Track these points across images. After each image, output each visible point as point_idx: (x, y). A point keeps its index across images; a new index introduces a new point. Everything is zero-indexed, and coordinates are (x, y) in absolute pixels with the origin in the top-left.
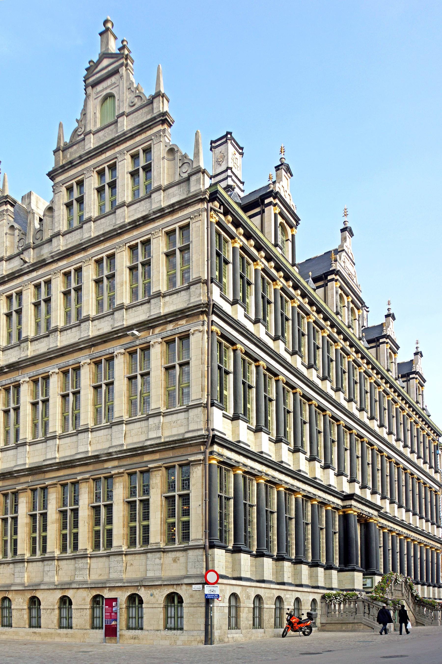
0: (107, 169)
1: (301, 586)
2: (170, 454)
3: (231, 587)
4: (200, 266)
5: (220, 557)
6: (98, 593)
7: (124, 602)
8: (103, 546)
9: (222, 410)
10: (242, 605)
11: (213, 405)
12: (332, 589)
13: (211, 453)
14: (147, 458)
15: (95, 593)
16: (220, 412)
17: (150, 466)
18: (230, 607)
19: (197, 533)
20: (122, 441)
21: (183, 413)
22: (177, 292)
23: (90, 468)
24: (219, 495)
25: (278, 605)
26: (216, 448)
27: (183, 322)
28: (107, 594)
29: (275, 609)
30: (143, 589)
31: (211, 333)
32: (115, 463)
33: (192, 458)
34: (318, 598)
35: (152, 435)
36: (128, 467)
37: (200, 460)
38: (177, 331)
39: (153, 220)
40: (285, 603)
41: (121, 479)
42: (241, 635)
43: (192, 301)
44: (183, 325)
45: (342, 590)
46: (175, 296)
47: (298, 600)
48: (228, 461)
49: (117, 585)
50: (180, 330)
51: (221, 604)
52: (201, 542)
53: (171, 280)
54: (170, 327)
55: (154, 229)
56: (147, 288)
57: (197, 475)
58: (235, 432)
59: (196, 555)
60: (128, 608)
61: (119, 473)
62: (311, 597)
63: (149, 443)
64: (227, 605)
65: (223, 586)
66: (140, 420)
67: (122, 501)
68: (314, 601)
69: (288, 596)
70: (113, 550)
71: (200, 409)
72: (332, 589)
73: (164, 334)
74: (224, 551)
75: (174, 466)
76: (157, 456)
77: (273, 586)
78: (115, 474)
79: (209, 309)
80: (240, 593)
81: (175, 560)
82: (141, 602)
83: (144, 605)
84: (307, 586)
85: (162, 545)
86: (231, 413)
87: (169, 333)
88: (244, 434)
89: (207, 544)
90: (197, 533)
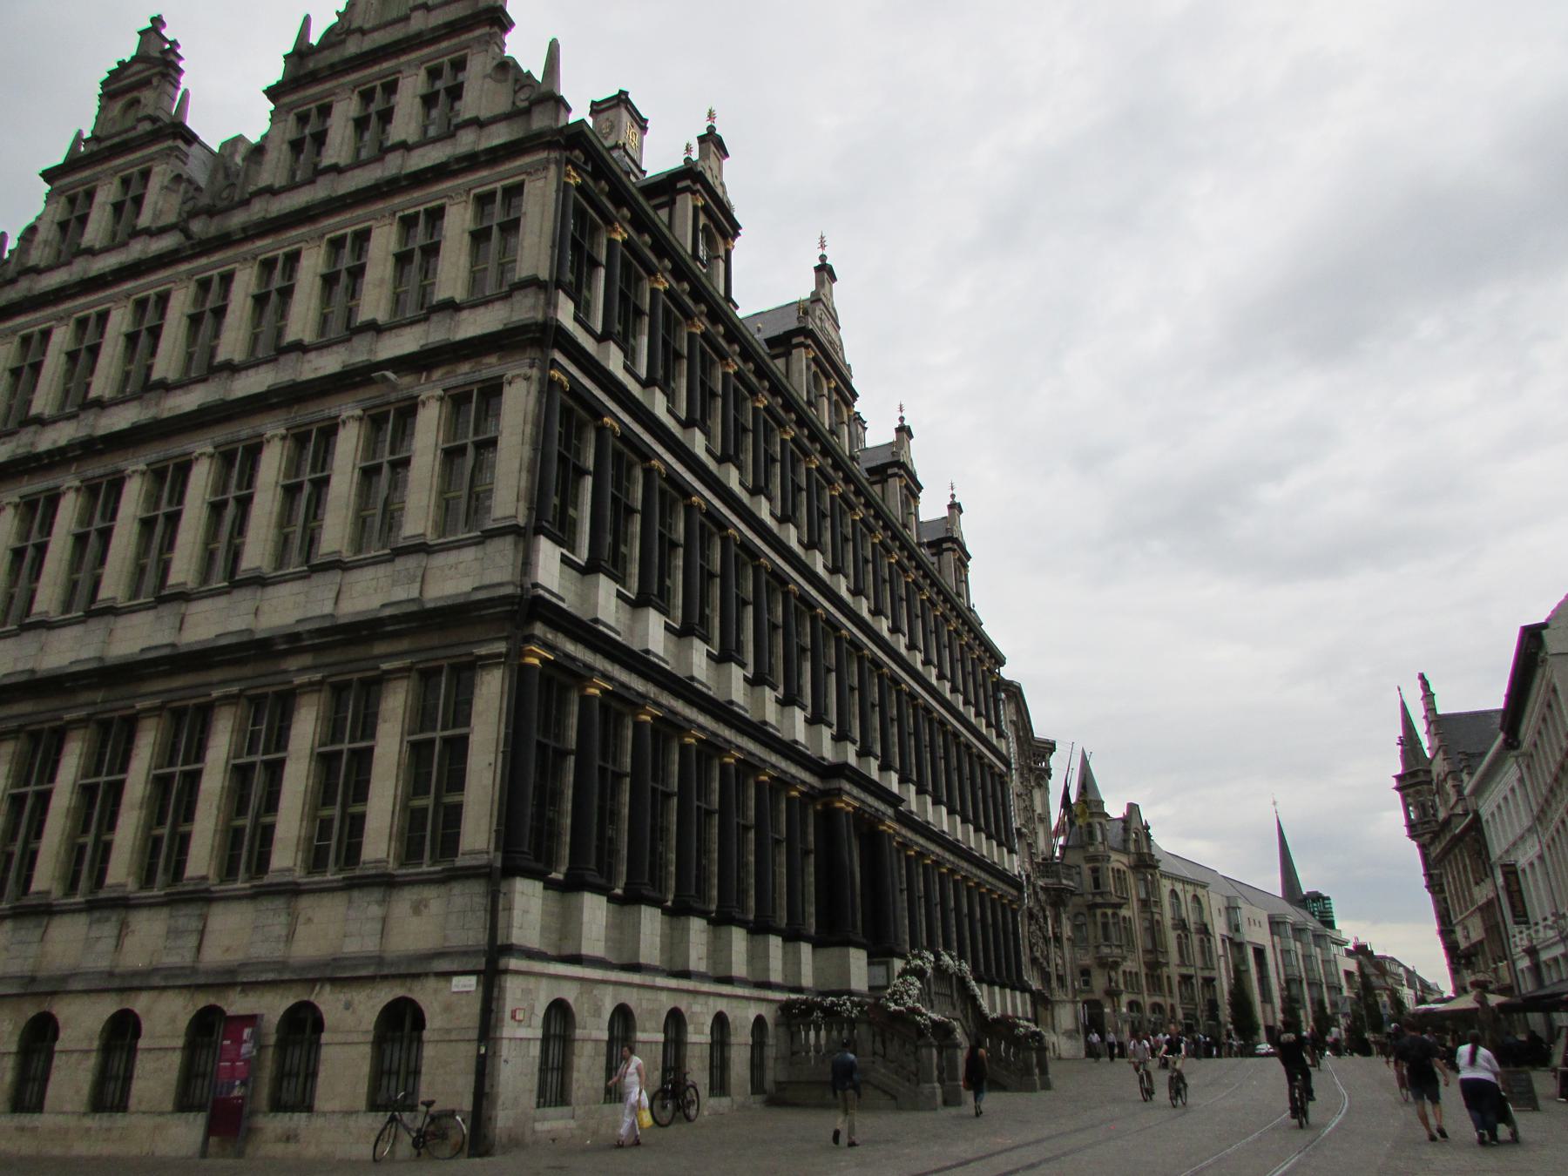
0: (379, 89)
1: (728, 980)
2: (434, 639)
3: (554, 983)
4: (534, 251)
5: (529, 903)
6: (212, 1000)
7: (273, 1029)
8: (248, 868)
9: (561, 545)
10: (579, 1033)
11: (539, 531)
12: (799, 990)
13: (530, 639)
14: (380, 648)
15: (203, 1001)
16: (558, 551)
17: (385, 666)
18: (546, 1040)
19: (477, 834)
20: (328, 608)
21: (473, 549)
22: (486, 302)
23: (247, 671)
24: (539, 743)
25: (672, 1034)
26: (539, 629)
27: (493, 360)
28: (237, 1004)
29: (665, 1044)
30: (328, 988)
31: (549, 386)
32: (307, 660)
33: (483, 651)
34: (768, 1013)
35: (400, 594)
36: (333, 670)
37: (499, 655)
38: (477, 376)
39: (454, 174)
40: (690, 1028)
41: (315, 697)
42: (572, 1124)
43: (515, 318)
44: (491, 366)
45: (826, 994)
46: (482, 310)
47: (720, 1021)
48: (568, 663)
49: (263, 977)
50: (486, 374)
51: (522, 1032)
52: (483, 860)
53: (475, 279)
54: (465, 367)
55: (452, 189)
56: (425, 291)
57: (491, 690)
58: (588, 597)
59: (468, 896)
60: (282, 1045)
61: (311, 684)
62: (752, 1011)
63: (387, 612)
64: (539, 1033)
65: (532, 980)
66: (376, 562)
67: (308, 751)
68: (759, 1020)
69: (697, 1008)
70: (267, 880)
71: (510, 539)
72: (799, 990)
73: (451, 382)
74: (539, 885)
75: (439, 670)
76: (404, 645)
77: (660, 981)
78: (301, 686)
79: (548, 336)
80: (576, 999)
81: (417, 909)
82: (319, 1025)
83: (325, 1037)
84: (743, 982)
85: (391, 867)
86: (582, 557)
87: (461, 380)
88: (605, 602)
89: (498, 864)
90: (477, 834)
